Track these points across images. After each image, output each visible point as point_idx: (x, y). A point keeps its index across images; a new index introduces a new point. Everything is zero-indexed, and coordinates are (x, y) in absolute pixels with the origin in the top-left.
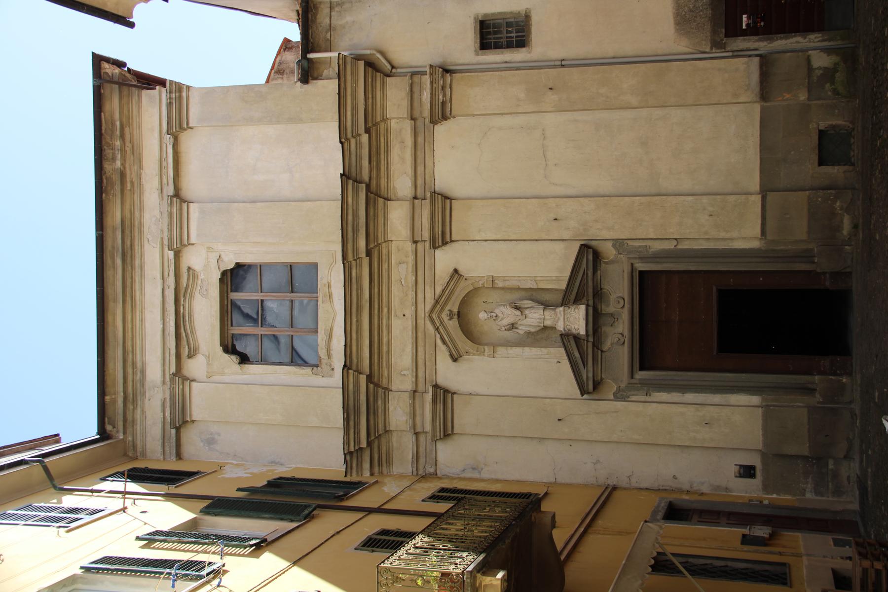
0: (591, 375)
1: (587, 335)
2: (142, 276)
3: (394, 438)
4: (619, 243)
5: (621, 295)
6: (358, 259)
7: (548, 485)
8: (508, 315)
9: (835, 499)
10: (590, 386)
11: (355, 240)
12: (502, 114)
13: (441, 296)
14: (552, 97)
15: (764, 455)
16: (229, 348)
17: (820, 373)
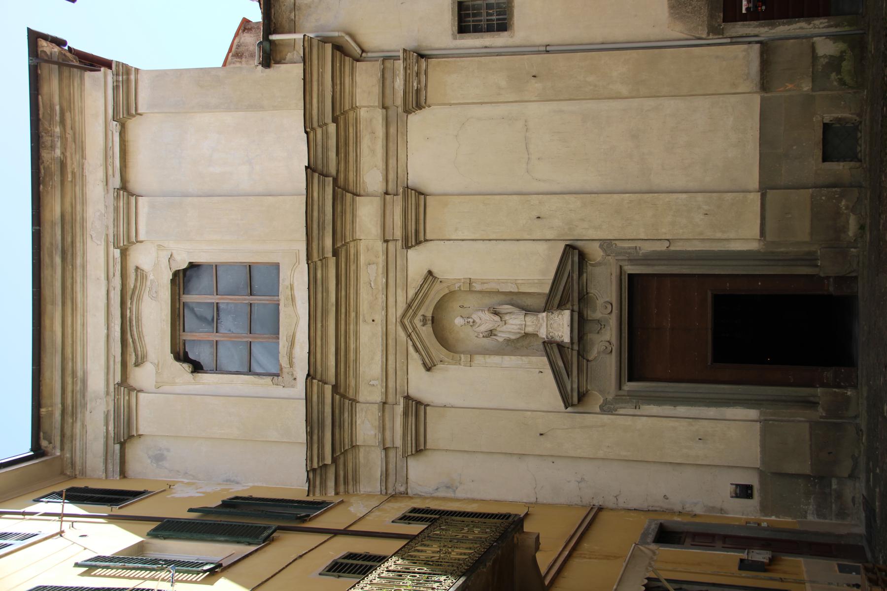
0: (575, 386)
1: (572, 342)
2: (84, 276)
3: (362, 454)
4: (607, 244)
5: (608, 300)
6: (323, 259)
7: (528, 505)
8: (486, 320)
9: (839, 522)
10: (574, 398)
11: (321, 238)
12: (482, 103)
13: (413, 300)
14: (536, 85)
15: (762, 474)
16: (181, 356)
17: (823, 385)
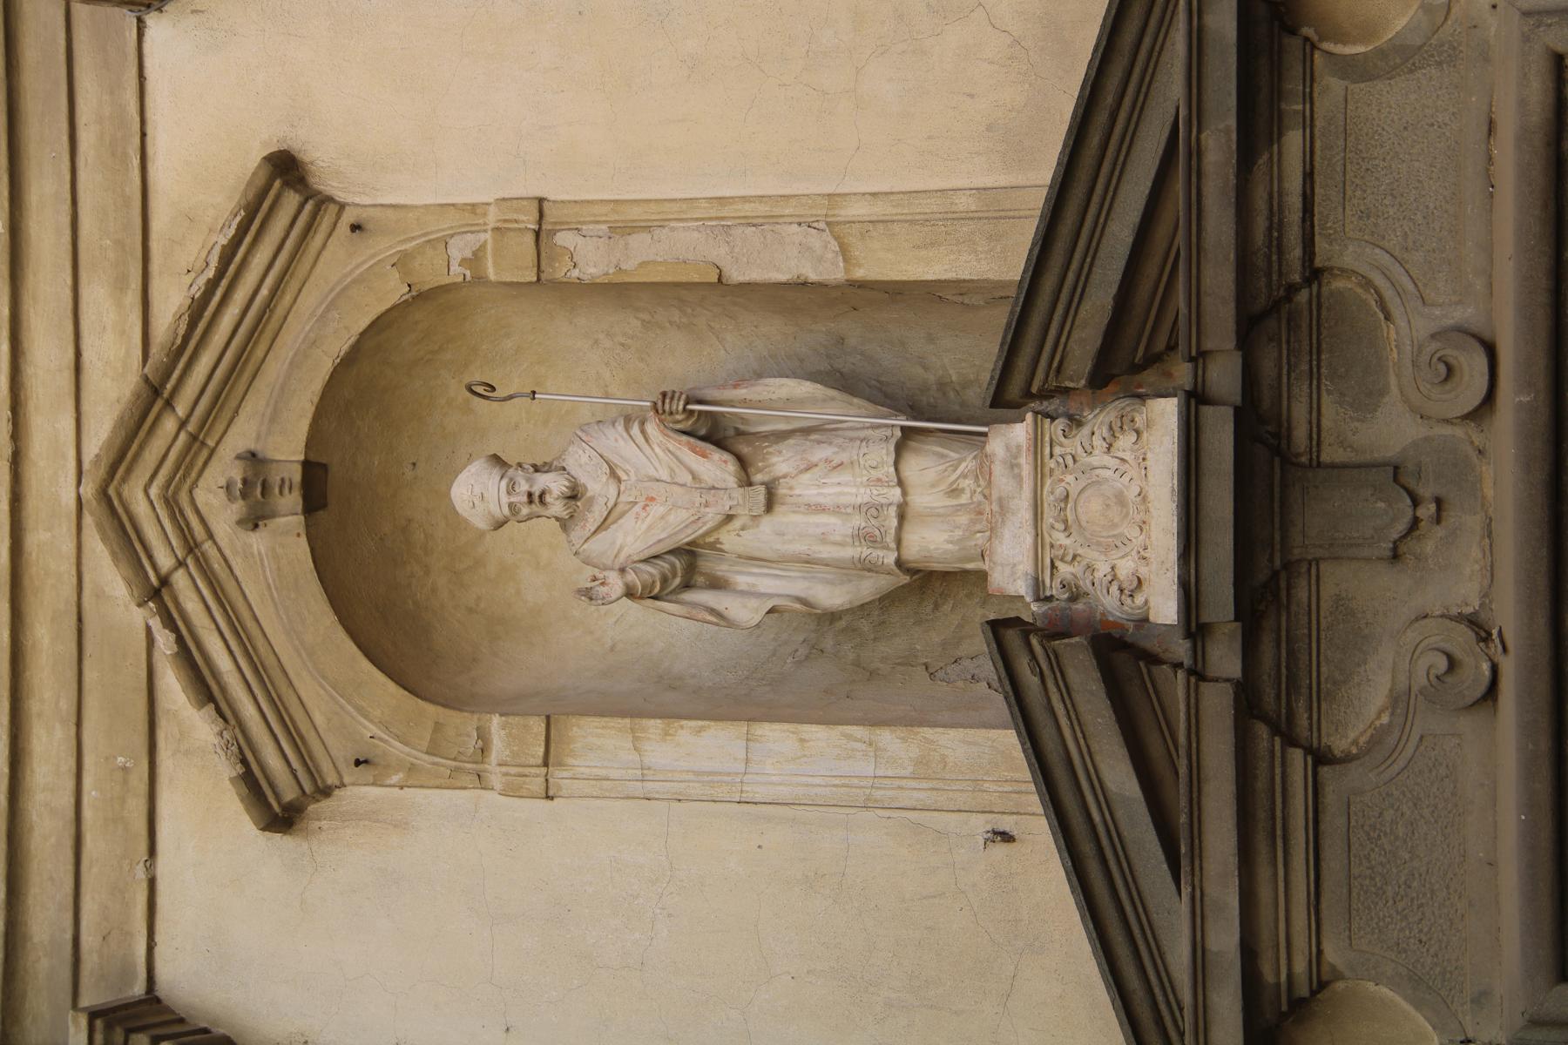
0: (1225, 939)
1: (1194, 626)
8: (655, 487)
